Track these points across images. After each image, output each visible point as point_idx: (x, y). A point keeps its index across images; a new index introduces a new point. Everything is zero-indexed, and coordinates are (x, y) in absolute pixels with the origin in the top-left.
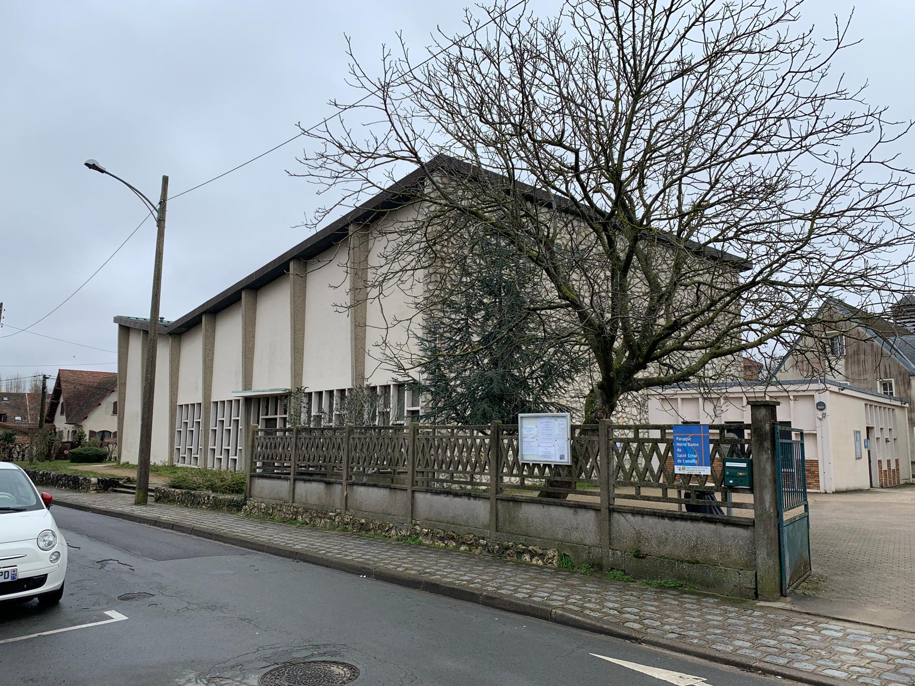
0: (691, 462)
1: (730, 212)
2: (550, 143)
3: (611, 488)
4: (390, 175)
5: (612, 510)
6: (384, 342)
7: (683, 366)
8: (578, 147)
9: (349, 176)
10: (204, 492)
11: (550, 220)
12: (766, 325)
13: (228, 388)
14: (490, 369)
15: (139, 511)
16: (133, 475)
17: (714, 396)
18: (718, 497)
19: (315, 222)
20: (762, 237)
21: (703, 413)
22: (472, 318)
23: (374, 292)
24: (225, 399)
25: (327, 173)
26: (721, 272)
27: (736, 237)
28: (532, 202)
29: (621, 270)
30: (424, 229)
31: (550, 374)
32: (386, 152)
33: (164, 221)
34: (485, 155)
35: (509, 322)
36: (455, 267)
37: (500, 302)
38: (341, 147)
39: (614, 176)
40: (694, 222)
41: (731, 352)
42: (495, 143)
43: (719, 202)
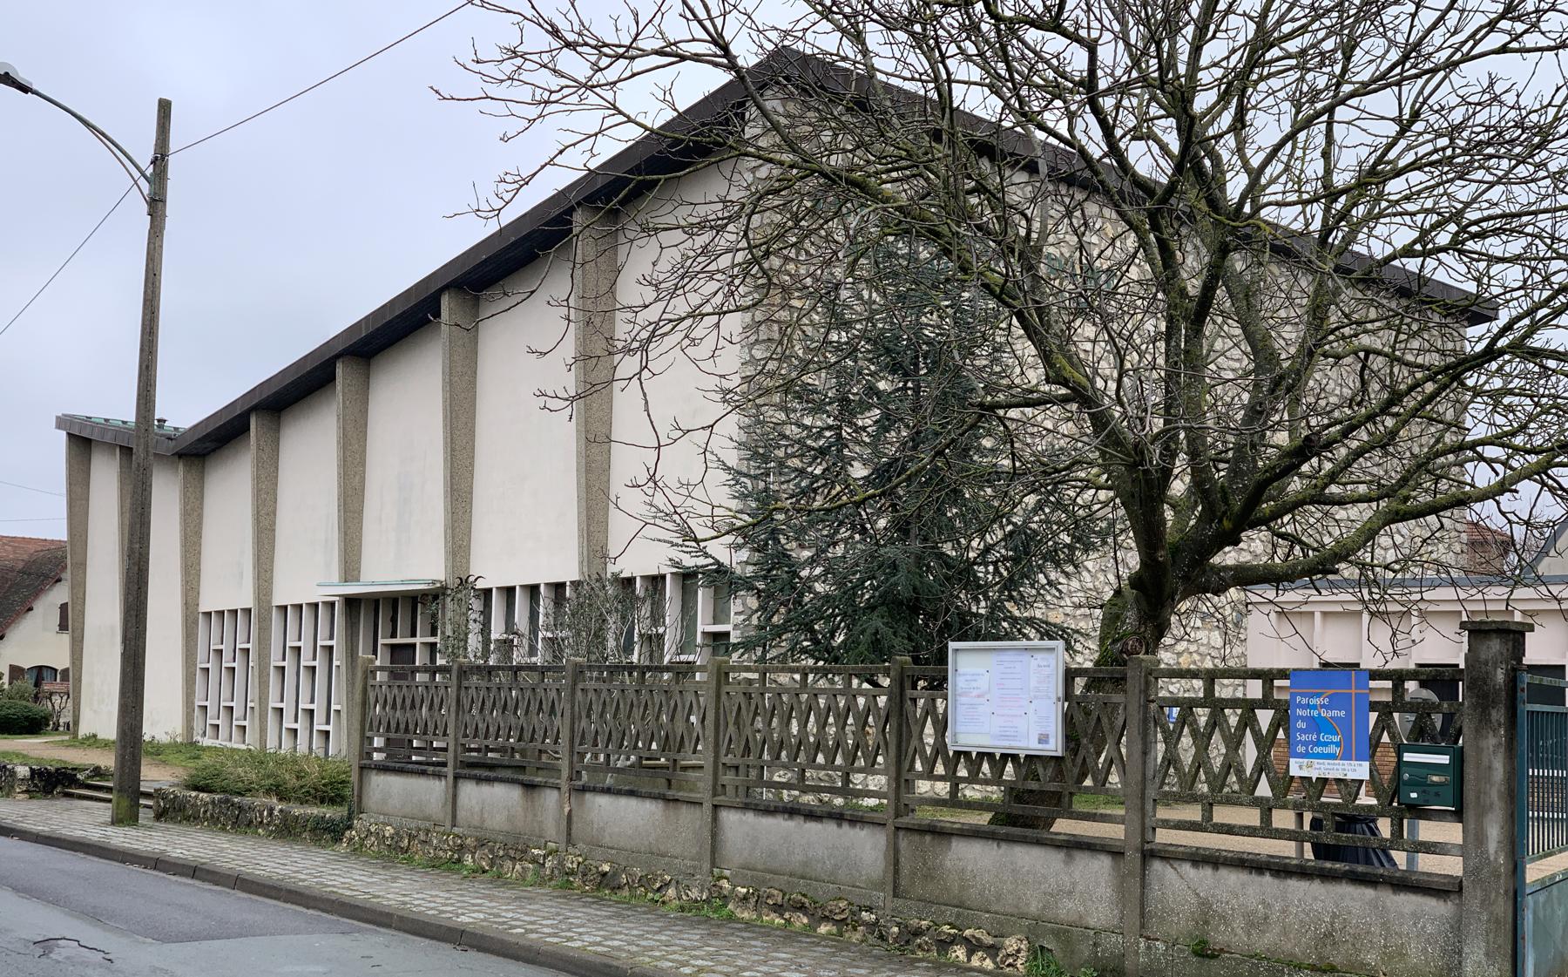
0: (1326, 750)
1: (1441, 190)
2: (1033, 24)
3: (1149, 806)
4: (667, 98)
5: (1150, 854)
6: (652, 478)
7: (1327, 540)
8: (1095, 34)
9: (574, 99)
10: (260, 801)
11: (1033, 200)
12: (1516, 449)
13: (309, 576)
14: (892, 541)
15: (120, 837)
16: (107, 761)
17: (1392, 607)
18: (1384, 827)
19: (498, 204)
20: (1516, 246)
21: (1369, 646)
22: (851, 424)
23: (628, 365)
24: (303, 601)
25: (525, 93)
26: (1415, 327)
27: (1456, 246)
28: (992, 160)
29: (1190, 316)
30: (744, 220)
31: (1027, 554)
32: (658, 44)
33: (163, 201)
34: (886, 51)
35: (937, 434)
36: (814, 308)
37: (917, 390)
38: (555, 32)
39: (1179, 102)
40: (1359, 211)
41: (1434, 509)
42: (909, 21)
43: (1415, 166)
